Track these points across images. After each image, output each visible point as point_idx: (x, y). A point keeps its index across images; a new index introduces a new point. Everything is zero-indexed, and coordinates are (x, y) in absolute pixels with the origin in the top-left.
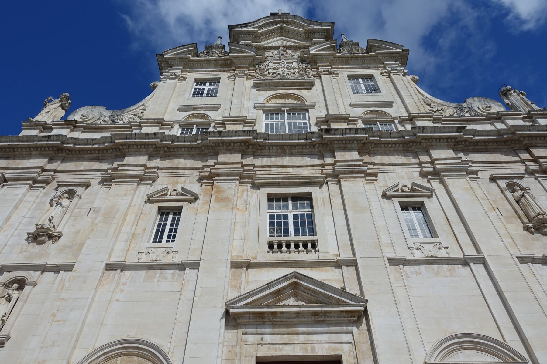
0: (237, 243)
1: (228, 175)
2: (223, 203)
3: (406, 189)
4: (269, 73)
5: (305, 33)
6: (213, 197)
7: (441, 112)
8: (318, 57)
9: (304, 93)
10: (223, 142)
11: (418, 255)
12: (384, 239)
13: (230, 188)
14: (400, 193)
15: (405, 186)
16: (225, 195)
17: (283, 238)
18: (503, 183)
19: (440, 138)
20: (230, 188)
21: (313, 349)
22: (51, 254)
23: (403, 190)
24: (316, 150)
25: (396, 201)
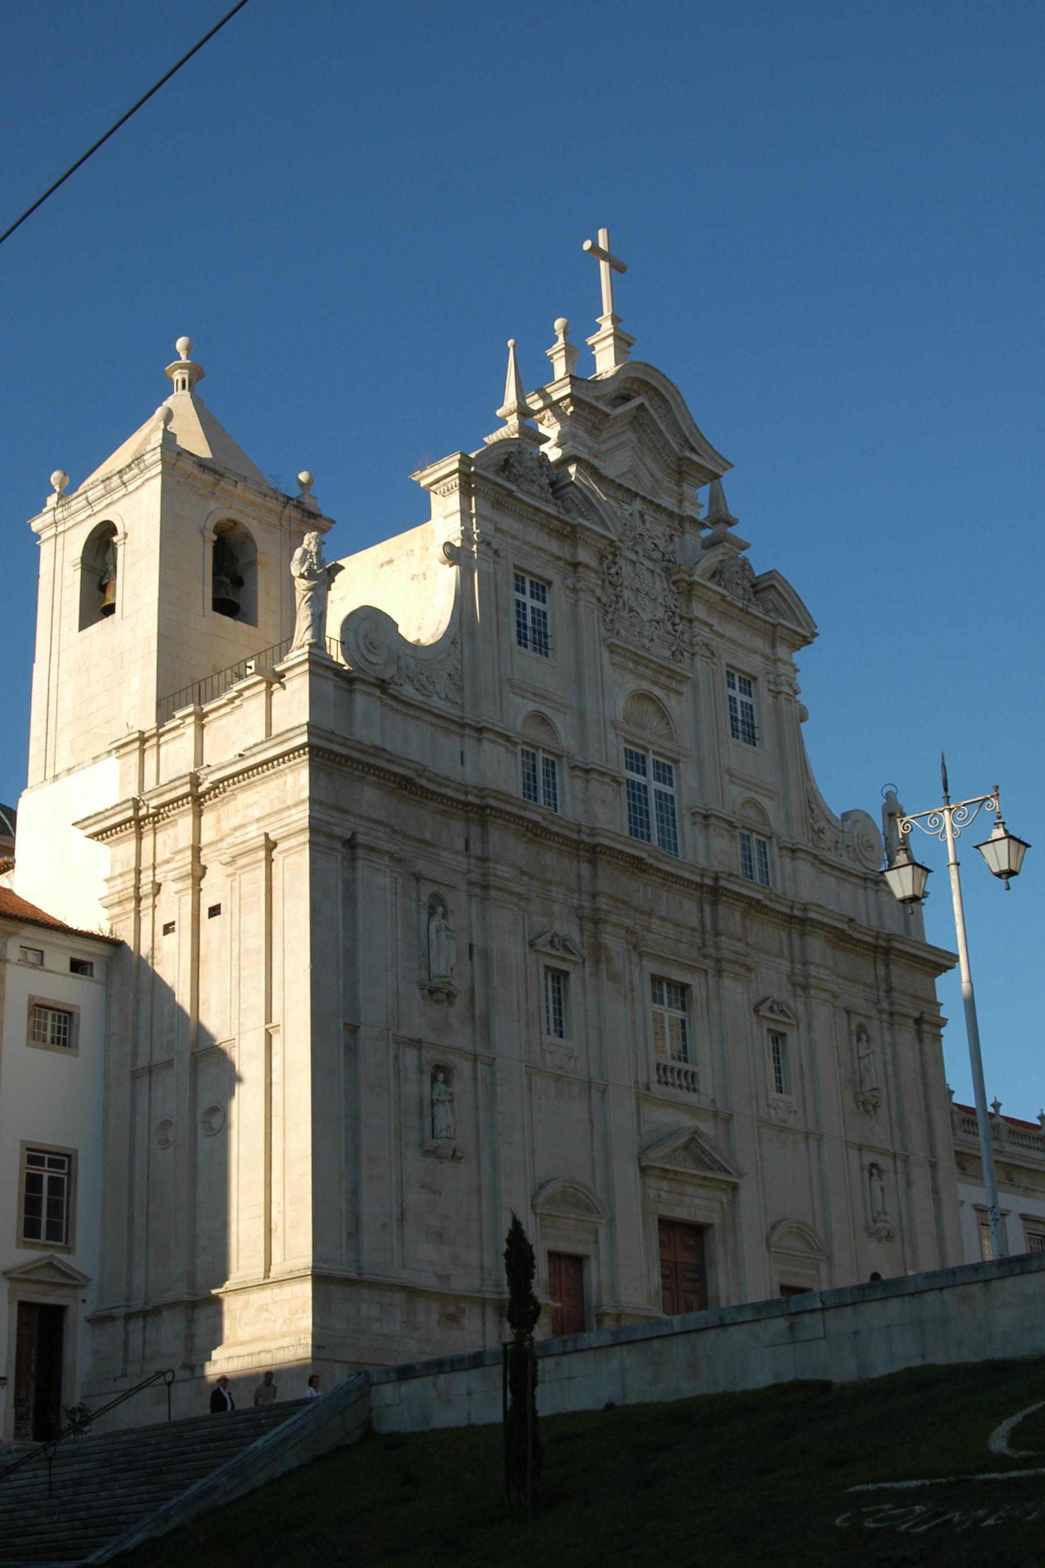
1: (615, 925)
3: (776, 1007)
5: (680, 459)
8: (700, 588)
10: (611, 849)
18: (855, 1021)
19: (826, 924)
25: (767, 1025)
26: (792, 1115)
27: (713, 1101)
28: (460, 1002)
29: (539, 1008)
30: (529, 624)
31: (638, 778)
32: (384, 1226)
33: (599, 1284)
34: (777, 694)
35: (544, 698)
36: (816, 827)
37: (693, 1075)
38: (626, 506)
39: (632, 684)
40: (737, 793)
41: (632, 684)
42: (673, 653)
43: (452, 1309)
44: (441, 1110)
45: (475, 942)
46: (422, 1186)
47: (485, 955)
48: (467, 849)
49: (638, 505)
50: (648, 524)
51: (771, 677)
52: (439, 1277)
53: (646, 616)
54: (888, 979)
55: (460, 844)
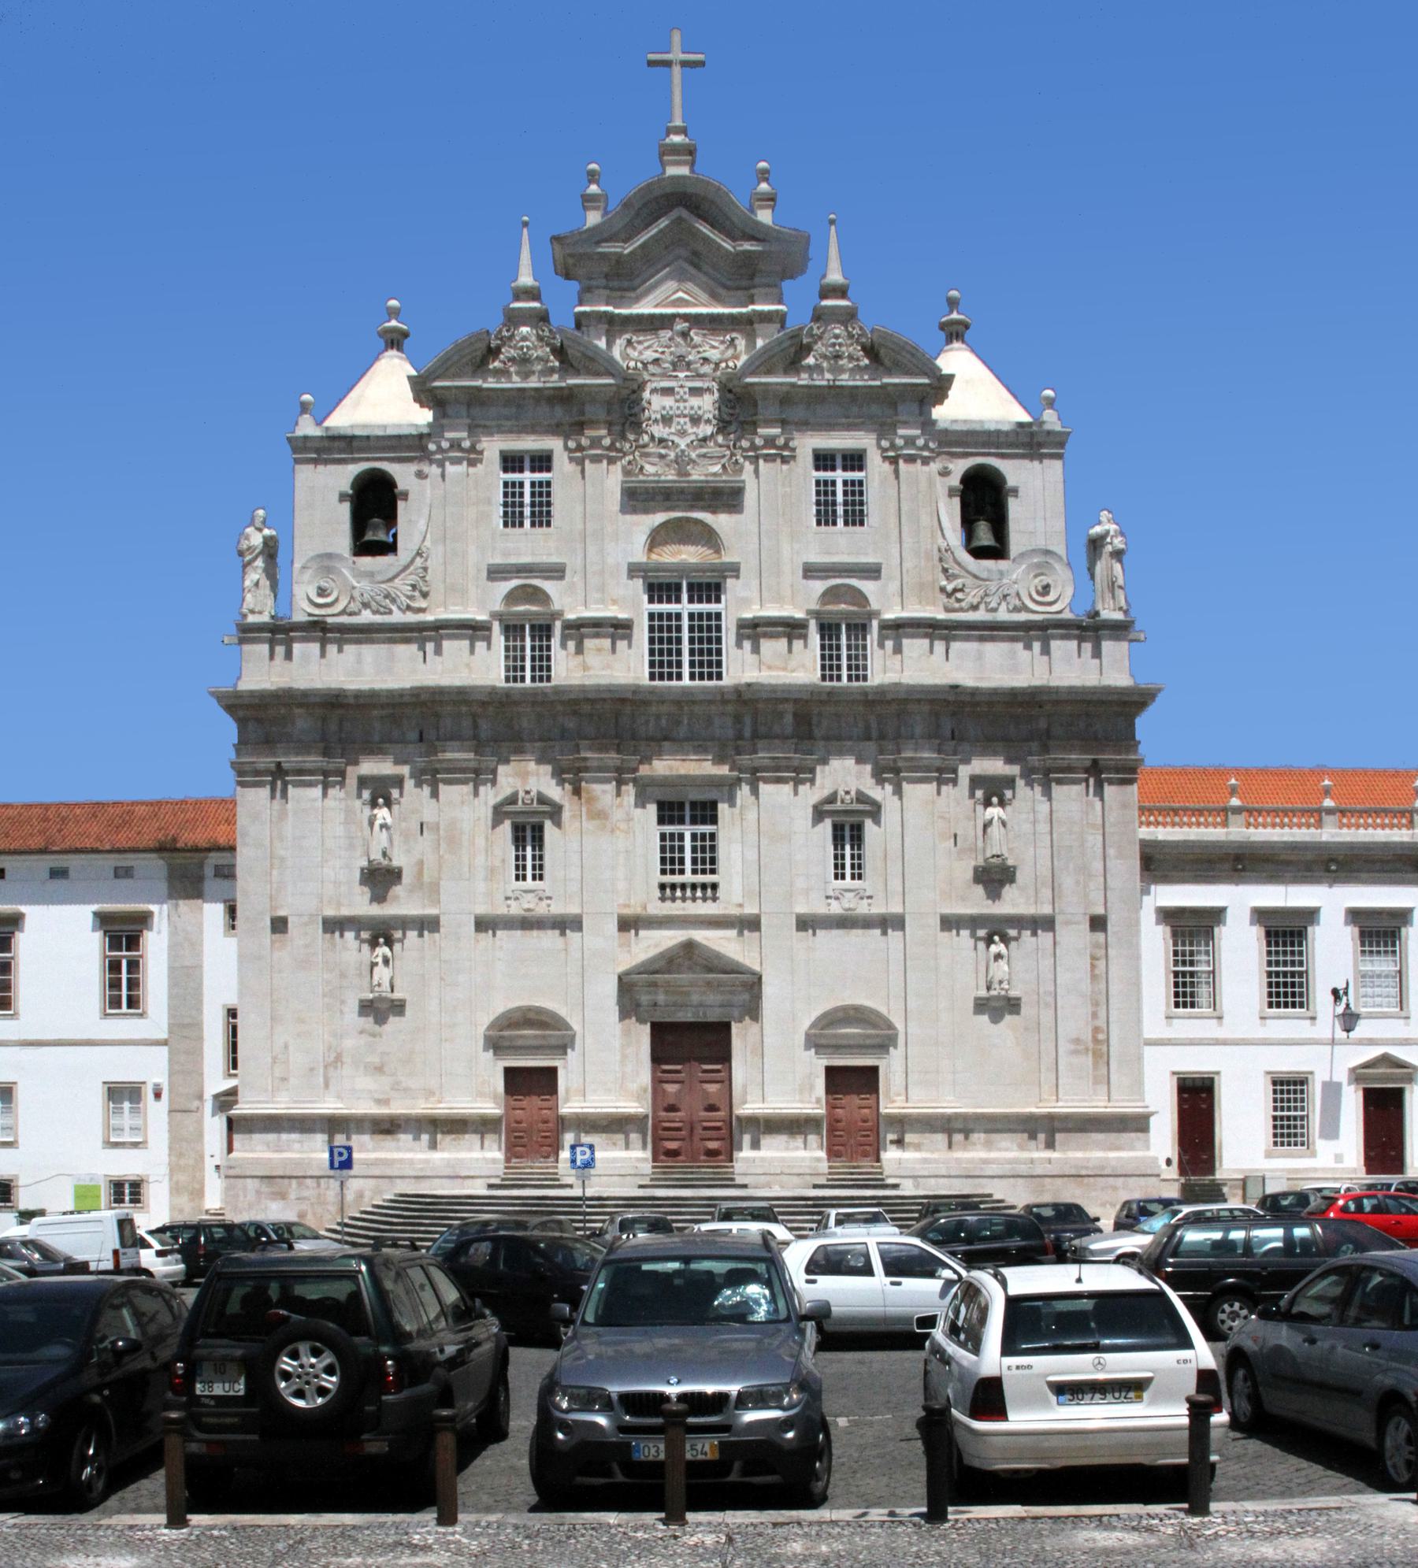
0: (621, 886)
2: (597, 822)
4: (652, 437)
6: (584, 809)
7: (959, 595)
9: (721, 521)
11: (836, 908)
12: (800, 883)
13: (604, 792)
14: (838, 806)
15: (847, 793)
16: (599, 806)
17: (677, 879)
20: (604, 792)
21: (705, 1014)
22: (403, 903)
23: (843, 802)
24: (730, 708)
26: (865, 901)
27: (741, 905)
28: (407, 878)
29: (503, 861)
30: (527, 499)
31: (672, 607)
32: (312, 1069)
33: (567, 1091)
34: (894, 461)
35: (531, 571)
36: (950, 588)
37: (714, 886)
38: (662, 333)
39: (660, 518)
40: (819, 586)
41: (660, 518)
42: (724, 466)
43: (387, 1126)
44: (376, 969)
45: (425, 820)
46: (361, 1032)
47: (436, 827)
48: (421, 740)
49: (680, 326)
50: (697, 339)
51: (885, 444)
52: (379, 1102)
53: (683, 443)
54: (1048, 731)
55: (413, 735)
